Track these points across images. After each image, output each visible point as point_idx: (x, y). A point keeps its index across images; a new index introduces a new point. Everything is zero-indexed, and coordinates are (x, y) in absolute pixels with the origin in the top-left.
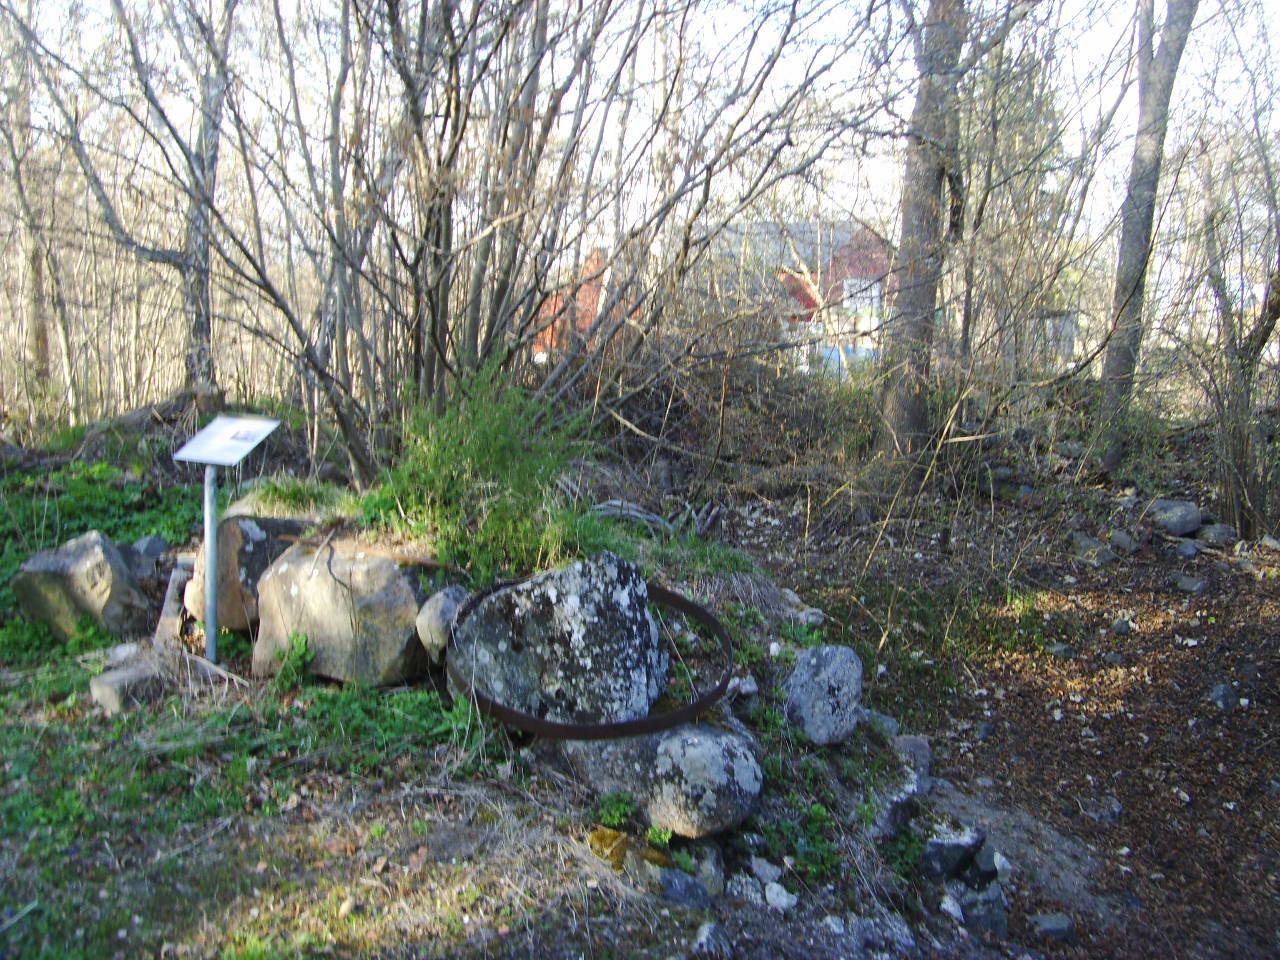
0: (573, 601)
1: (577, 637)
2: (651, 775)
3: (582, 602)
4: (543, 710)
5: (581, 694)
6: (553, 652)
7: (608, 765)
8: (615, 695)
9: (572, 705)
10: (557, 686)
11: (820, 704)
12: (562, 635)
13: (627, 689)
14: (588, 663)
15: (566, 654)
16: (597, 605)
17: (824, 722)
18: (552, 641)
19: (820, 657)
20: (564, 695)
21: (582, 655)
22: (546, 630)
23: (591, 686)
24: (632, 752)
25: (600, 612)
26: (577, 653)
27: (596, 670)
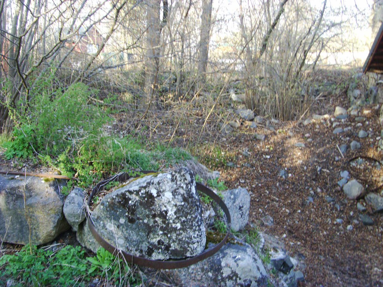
0: (168, 195)
1: (171, 213)
2: (220, 278)
3: (173, 195)
4: (150, 252)
5: (174, 241)
6: (155, 222)
7: (193, 275)
8: (195, 240)
9: (168, 247)
10: (158, 239)
11: (236, 214)
12: (161, 212)
13: (200, 236)
14: (179, 226)
15: (164, 222)
16: (183, 195)
17: (238, 222)
18: (154, 216)
19: (235, 195)
20: (163, 243)
21: (174, 222)
22: (150, 211)
23: (180, 237)
24: (205, 267)
25: (185, 200)
26: (171, 221)
27: (183, 229)
